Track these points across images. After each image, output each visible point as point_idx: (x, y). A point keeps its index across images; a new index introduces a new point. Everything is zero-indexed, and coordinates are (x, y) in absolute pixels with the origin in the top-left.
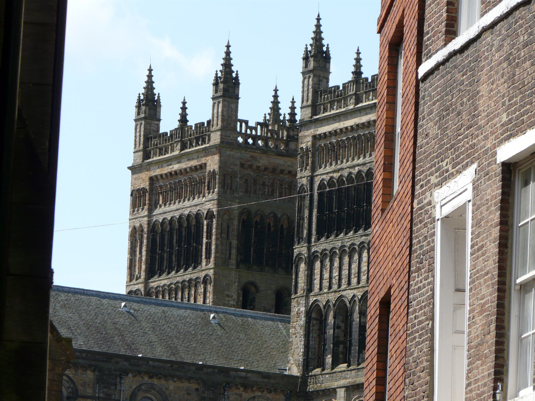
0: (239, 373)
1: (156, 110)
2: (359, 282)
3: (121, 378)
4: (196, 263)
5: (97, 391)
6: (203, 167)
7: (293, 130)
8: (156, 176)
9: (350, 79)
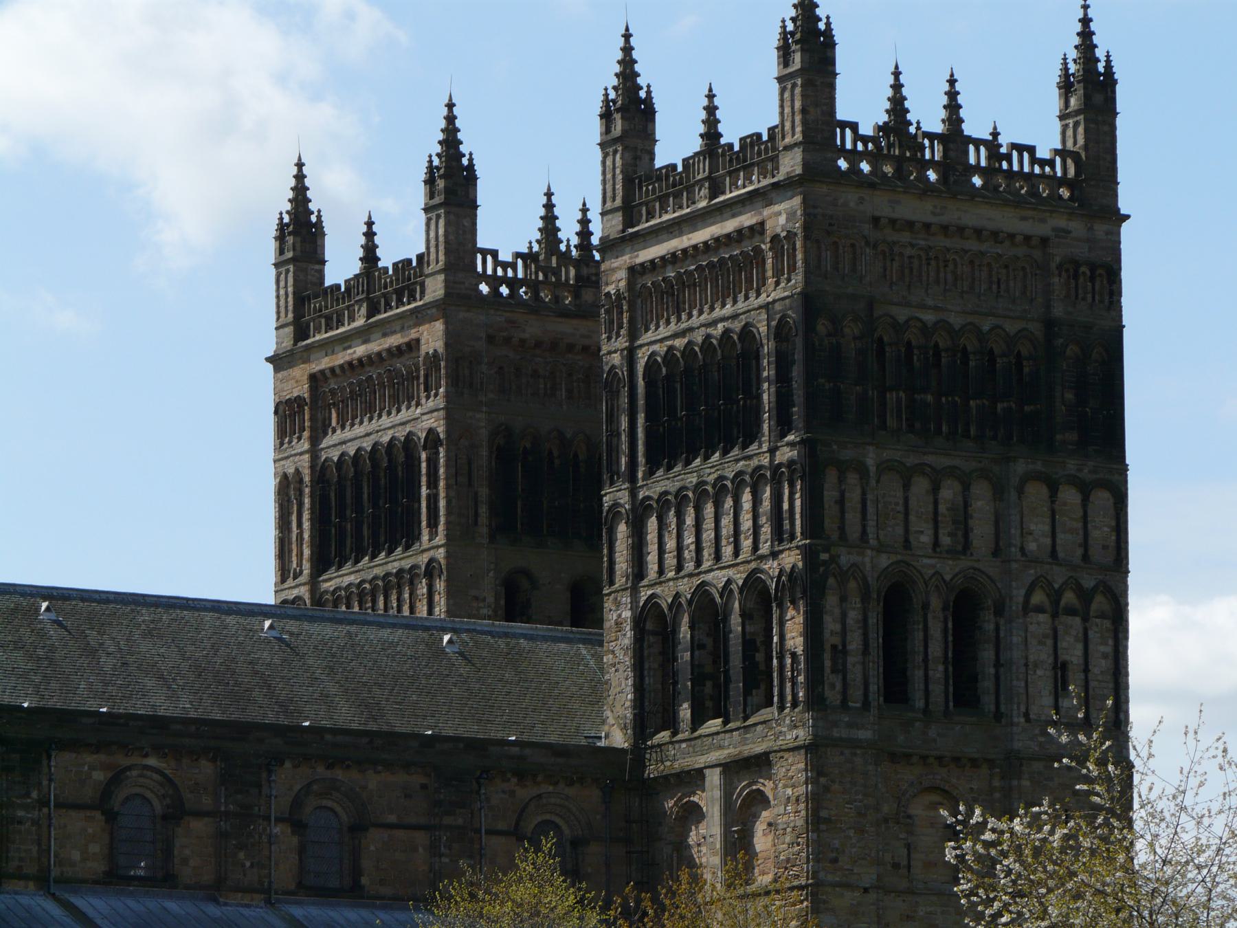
0: (506, 748)
1: (315, 242)
2: (736, 553)
3: (270, 772)
4: (410, 537)
5: (223, 801)
6: (413, 346)
7: (587, 265)
8: (322, 372)
9: (698, 149)
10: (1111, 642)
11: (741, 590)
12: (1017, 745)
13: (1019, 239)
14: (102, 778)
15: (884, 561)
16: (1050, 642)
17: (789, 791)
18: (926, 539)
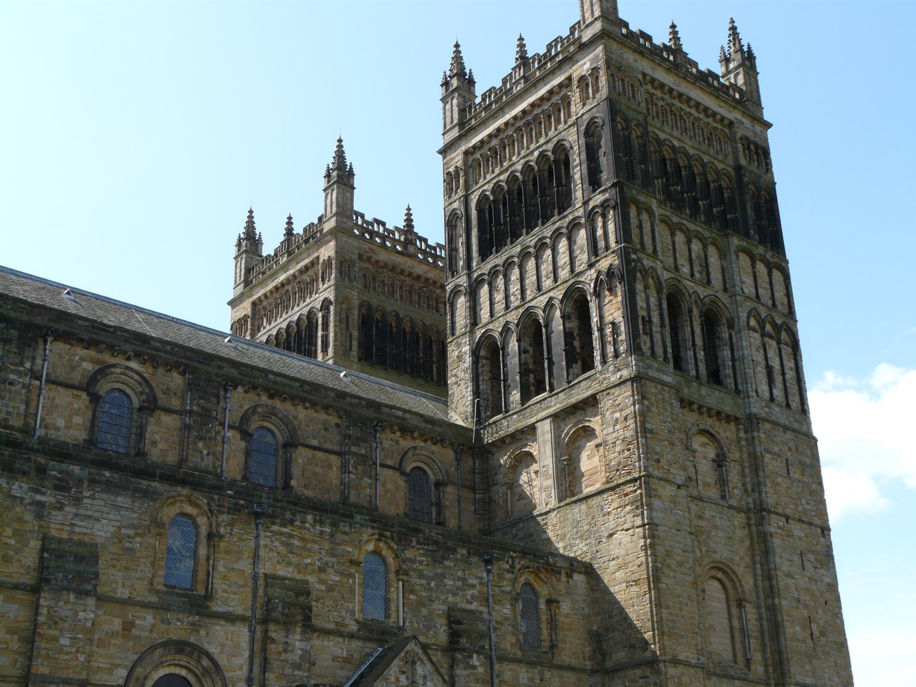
1: (257, 247)
3: (226, 390)
5: (189, 402)
6: (313, 263)
7: (411, 234)
10: (793, 361)
11: (562, 302)
12: (754, 410)
13: (718, 117)
14: (90, 368)
15: (665, 275)
16: (762, 351)
17: (617, 415)
18: (686, 270)
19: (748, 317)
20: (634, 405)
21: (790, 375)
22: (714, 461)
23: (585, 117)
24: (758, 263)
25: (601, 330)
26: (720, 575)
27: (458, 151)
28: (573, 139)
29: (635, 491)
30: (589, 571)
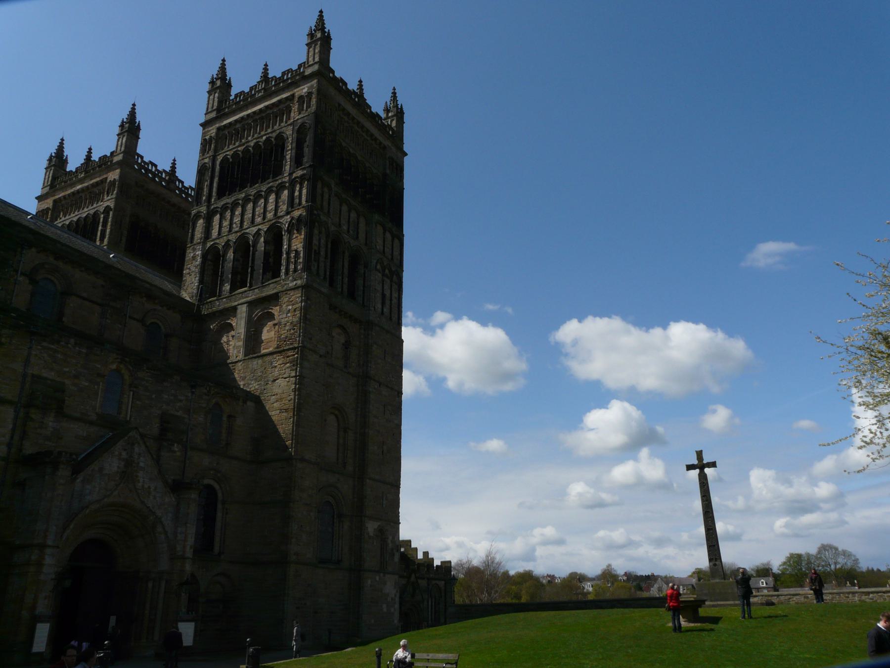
10: (397, 293)
11: (266, 232)
16: (381, 284)
18: (345, 228)
19: (377, 263)
20: (301, 302)
21: (395, 301)
22: (343, 344)
23: (299, 121)
24: (387, 232)
25: (288, 254)
26: (337, 412)
27: (214, 127)
28: (289, 132)
29: (294, 355)
30: (257, 400)
